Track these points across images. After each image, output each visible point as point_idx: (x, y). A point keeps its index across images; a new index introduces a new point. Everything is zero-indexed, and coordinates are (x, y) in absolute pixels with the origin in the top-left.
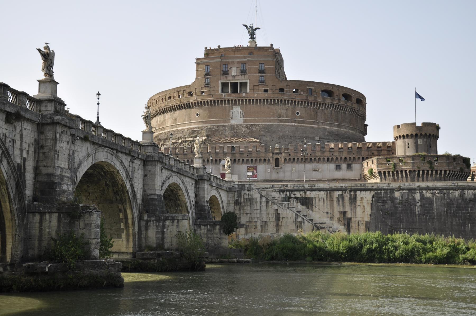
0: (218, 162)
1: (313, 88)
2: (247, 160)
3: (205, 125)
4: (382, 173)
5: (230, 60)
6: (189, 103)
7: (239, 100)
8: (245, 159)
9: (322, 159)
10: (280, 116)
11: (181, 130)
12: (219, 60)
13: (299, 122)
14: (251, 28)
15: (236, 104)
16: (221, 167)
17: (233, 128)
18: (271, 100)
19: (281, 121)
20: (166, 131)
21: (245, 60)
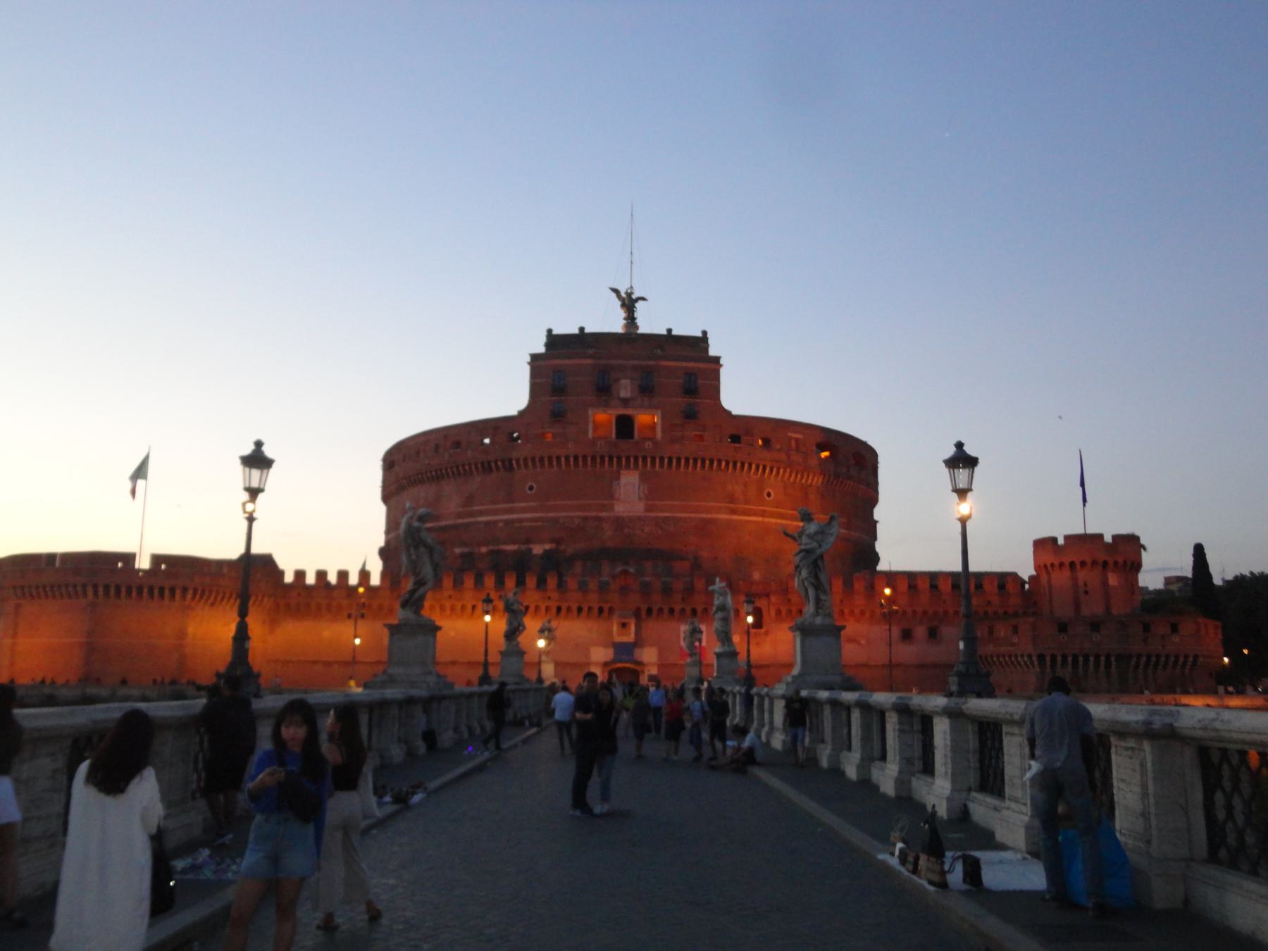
0: (605, 614)
1: (800, 436)
2: (683, 610)
3: (551, 515)
4: (1048, 659)
5: (614, 362)
6: (510, 460)
7: (636, 458)
8: (677, 608)
9: (868, 614)
10: (732, 499)
11: (487, 523)
12: (589, 361)
13: (772, 515)
14: (629, 295)
15: (628, 467)
16: (615, 628)
17: (620, 523)
18: (712, 461)
19: (733, 512)
20: (443, 523)
21: (652, 363)
